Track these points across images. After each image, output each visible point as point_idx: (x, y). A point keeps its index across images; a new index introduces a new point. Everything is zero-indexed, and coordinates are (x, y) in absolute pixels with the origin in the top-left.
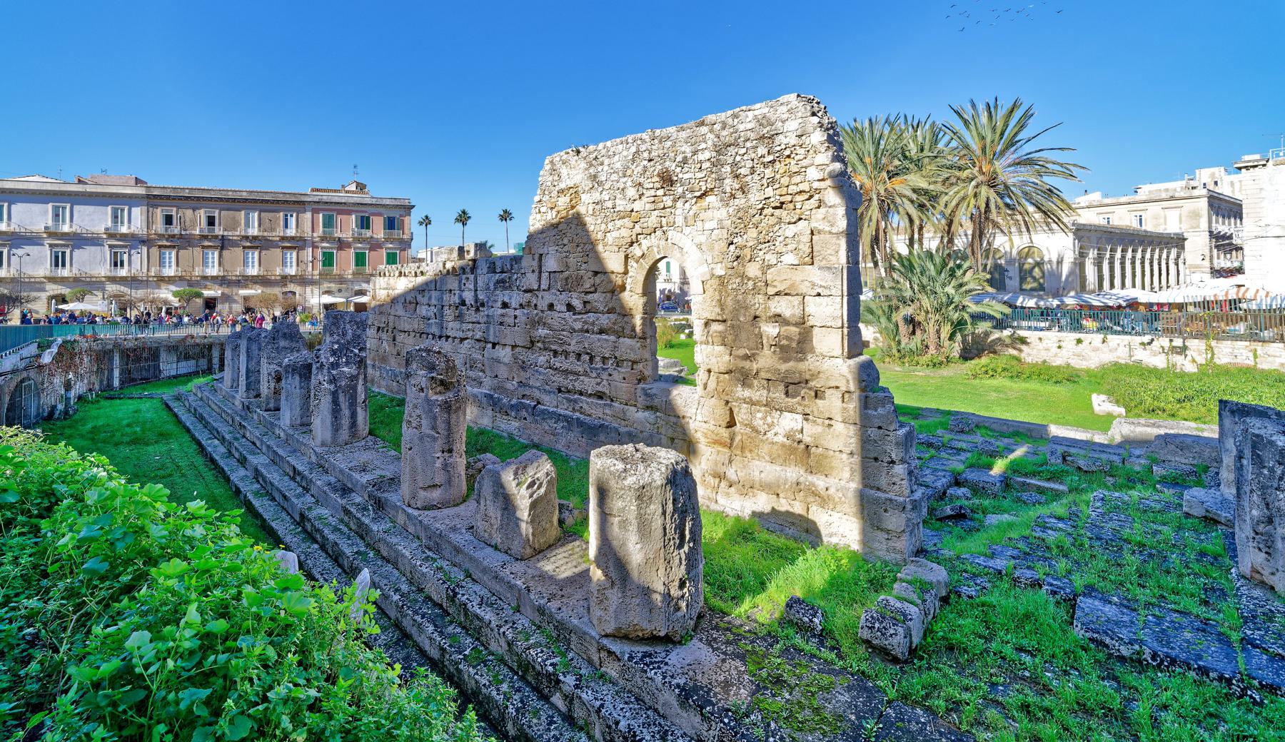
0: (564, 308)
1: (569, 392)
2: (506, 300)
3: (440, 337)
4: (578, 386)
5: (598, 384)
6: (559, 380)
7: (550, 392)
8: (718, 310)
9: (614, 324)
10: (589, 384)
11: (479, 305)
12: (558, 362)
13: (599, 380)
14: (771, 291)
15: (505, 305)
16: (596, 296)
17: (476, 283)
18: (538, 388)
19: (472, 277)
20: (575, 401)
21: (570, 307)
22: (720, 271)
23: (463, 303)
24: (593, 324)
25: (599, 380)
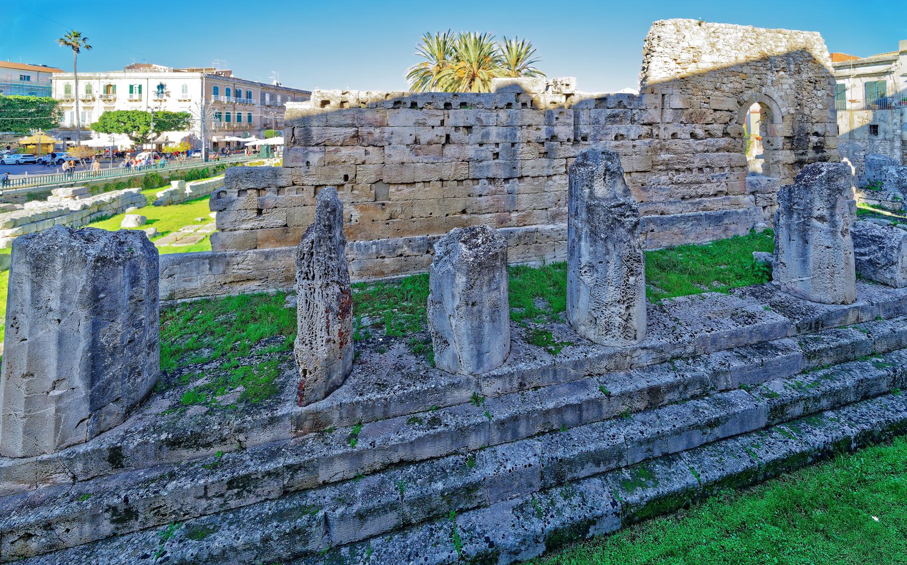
0: (688, 136)
1: (691, 197)
4: (700, 191)
5: (718, 186)
6: (683, 191)
7: (675, 202)
8: (792, 131)
9: (729, 144)
10: (711, 188)
12: (680, 177)
13: (719, 183)
14: (814, 121)
16: (715, 126)
18: (663, 202)
20: (699, 203)
21: (693, 136)
22: (792, 111)
24: (713, 146)
25: (719, 183)
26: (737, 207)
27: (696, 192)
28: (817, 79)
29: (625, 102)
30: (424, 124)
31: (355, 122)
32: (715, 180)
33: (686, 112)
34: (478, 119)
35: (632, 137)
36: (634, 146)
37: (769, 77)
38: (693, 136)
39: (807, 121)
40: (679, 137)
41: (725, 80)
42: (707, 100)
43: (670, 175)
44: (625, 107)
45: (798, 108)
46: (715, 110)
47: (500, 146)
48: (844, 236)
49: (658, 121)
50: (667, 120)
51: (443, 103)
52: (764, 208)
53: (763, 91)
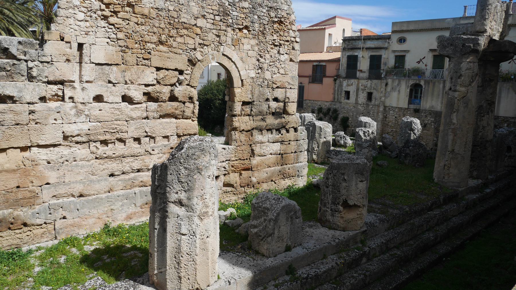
8: (250, 96)
9: (176, 109)
12: (108, 150)
14: (275, 86)
21: (126, 99)
27: (130, 167)
28: (281, 42)
32: (156, 151)
36: (32, 112)
38: (126, 99)
40: (105, 100)
41: (173, 32)
42: (147, 56)
43: (93, 149)
45: (260, 71)
46: (158, 69)
50: (85, 78)
53: (222, 50)
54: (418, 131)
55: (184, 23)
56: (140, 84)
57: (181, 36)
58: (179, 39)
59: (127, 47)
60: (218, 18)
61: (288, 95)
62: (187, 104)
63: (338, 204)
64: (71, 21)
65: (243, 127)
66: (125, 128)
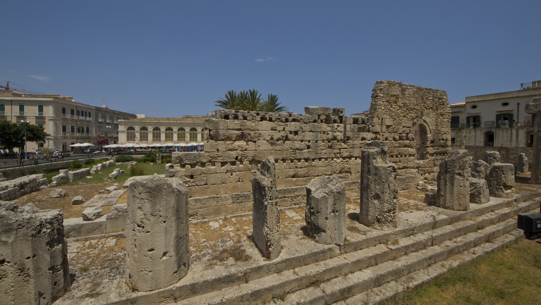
0: (392, 139)
2: (365, 136)
3: (313, 160)
11: (346, 139)
14: (442, 133)
15: (363, 139)
17: (345, 128)
19: (342, 125)
21: (394, 139)
23: (335, 138)
26: (411, 174)
28: (444, 113)
29: (366, 121)
30: (275, 130)
31: (242, 127)
33: (391, 127)
34: (301, 128)
35: (369, 139)
37: (426, 111)
38: (394, 139)
39: (440, 133)
41: (408, 112)
42: (400, 122)
44: (366, 124)
46: (404, 127)
47: (311, 142)
48: (467, 181)
49: (380, 131)
50: (383, 131)
51: (284, 118)
52: (422, 175)
54: (499, 159)
55: (411, 108)
56: (398, 133)
57: (410, 113)
58: (410, 114)
59: (395, 119)
60: (422, 105)
61: (448, 137)
62: (412, 141)
63: (500, 185)
64: (380, 110)
65: (431, 152)
66: (394, 151)
